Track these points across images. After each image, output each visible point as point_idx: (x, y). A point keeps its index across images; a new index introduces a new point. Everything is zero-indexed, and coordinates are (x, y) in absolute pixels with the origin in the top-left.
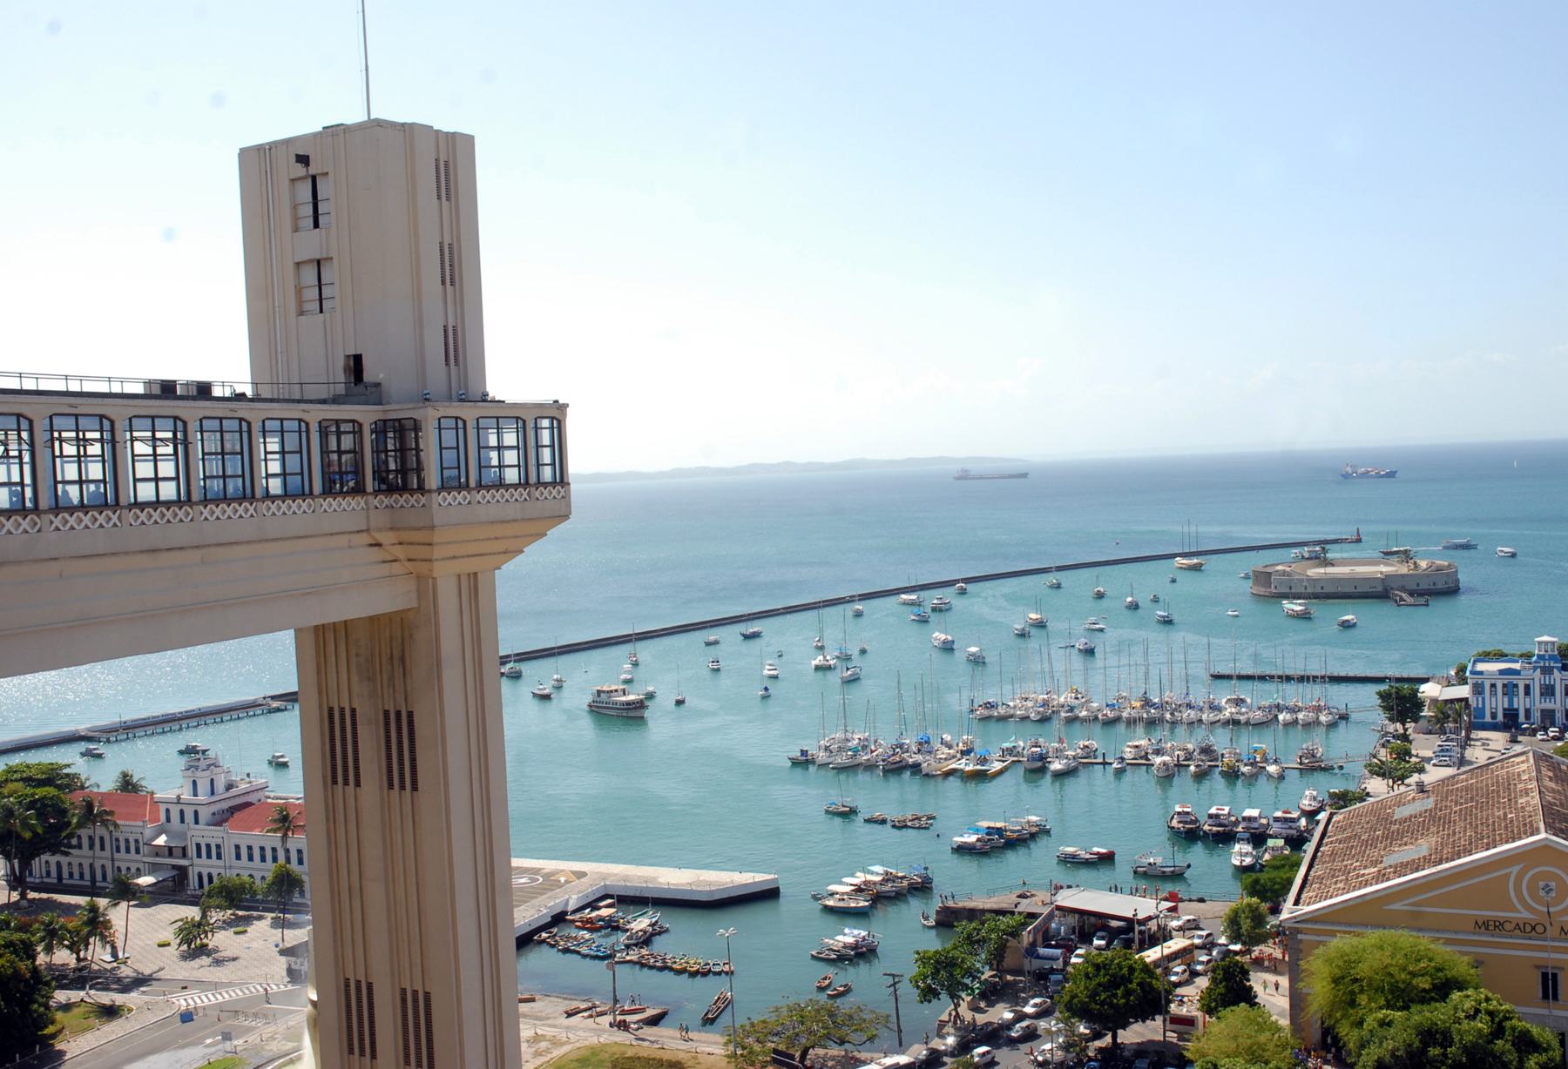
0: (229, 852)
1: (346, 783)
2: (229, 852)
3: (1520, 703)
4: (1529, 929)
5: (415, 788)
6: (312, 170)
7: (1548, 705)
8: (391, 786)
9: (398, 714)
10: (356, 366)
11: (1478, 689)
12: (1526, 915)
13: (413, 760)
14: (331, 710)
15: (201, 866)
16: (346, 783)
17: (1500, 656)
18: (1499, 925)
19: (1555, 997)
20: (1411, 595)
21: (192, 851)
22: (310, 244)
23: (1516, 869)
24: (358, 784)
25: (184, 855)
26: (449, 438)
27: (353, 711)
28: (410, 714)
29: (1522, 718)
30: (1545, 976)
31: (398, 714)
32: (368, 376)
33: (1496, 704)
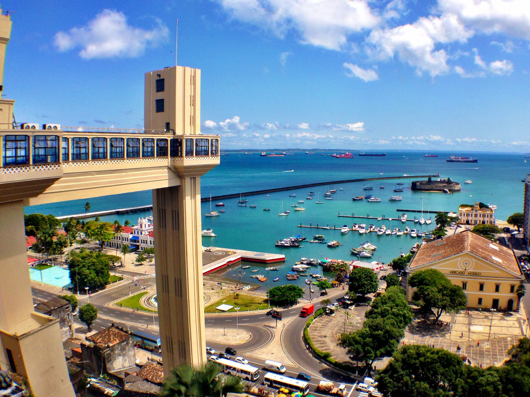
0: (149, 242)
2: (149, 242)
3: (470, 218)
4: (462, 273)
7: (476, 219)
8: (173, 229)
10: (168, 124)
11: (461, 215)
12: (461, 270)
13: (178, 223)
14: (160, 210)
15: (142, 245)
17: (466, 206)
18: (455, 272)
19: (465, 289)
21: (140, 242)
23: (460, 259)
24: (165, 228)
25: (138, 242)
26: (189, 144)
29: (470, 222)
30: (464, 284)
32: (171, 128)
33: (464, 219)
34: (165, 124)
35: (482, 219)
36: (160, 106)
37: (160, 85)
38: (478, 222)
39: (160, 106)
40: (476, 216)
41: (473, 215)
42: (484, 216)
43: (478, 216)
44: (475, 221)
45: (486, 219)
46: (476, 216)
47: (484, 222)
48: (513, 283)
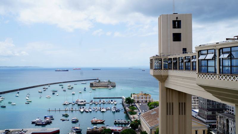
1: (170, 114)
3: (139, 100)
5: (185, 114)
6: (178, 20)
7: (142, 100)
8: (180, 114)
9: (182, 103)
10: (185, 50)
11: (134, 98)
16: (170, 114)
20: (112, 87)
22: (177, 31)
24: (172, 114)
27: (172, 103)
28: (185, 103)
31: (182, 103)
34: (182, 49)
35: (145, 100)
36: (177, 37)
37: (177, 24)
38: (143, 102)
39: (177, 37)
40: (142, 98)
41: (141, 98)
42: (146, 98)
43: (143, 98)
44: (142, 101)
45: (147, 99)
46: (142, 98)
47: (146, 101)
48: (204, 129)
